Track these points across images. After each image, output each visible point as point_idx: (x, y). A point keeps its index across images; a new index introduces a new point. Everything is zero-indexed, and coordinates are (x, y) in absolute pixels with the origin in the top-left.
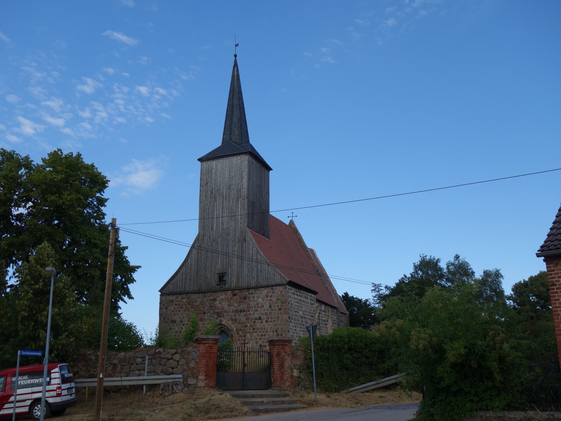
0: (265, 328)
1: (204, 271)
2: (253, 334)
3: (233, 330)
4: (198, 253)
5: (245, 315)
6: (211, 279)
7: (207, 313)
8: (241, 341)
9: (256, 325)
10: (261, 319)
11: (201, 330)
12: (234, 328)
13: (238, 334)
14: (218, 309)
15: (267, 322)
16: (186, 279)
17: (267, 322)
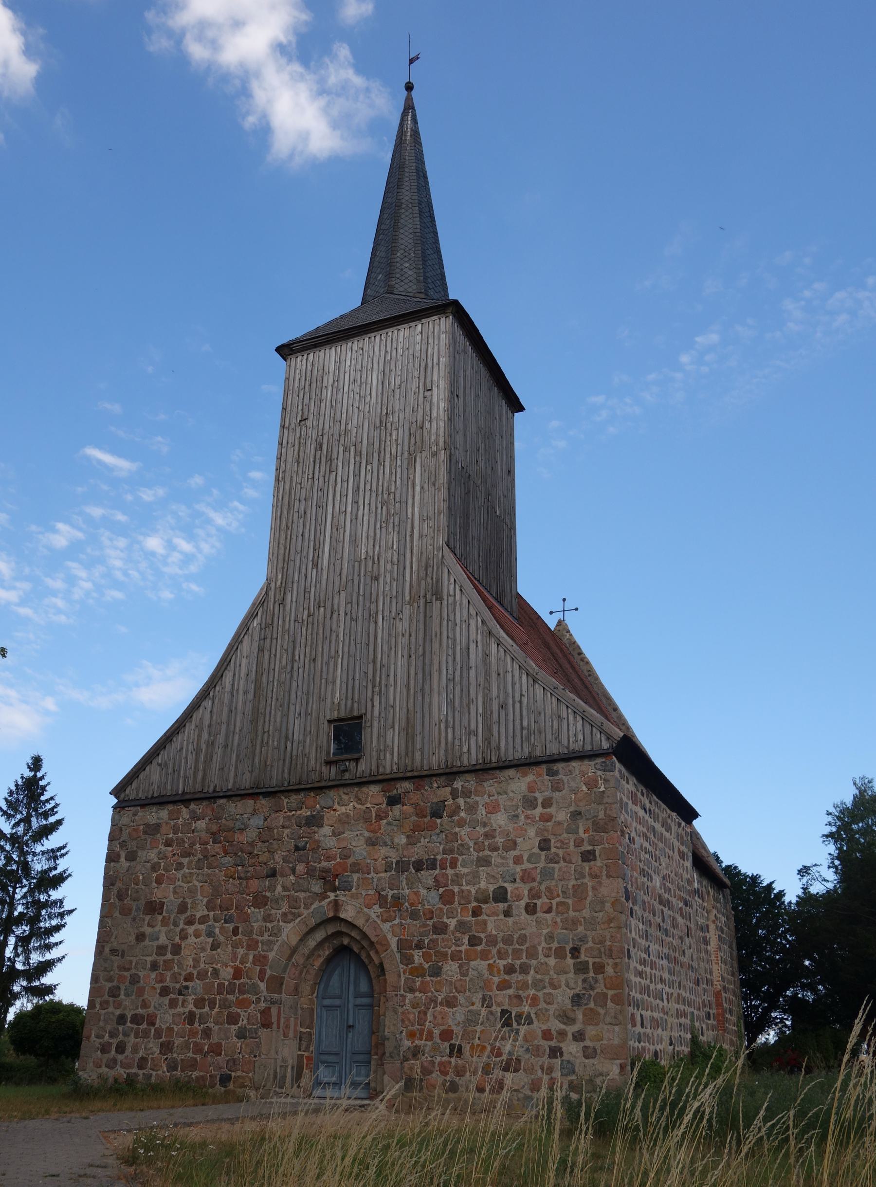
0: (523, 939)
1: (279, 714)
2: (472, 963)
3: (386, 945)
4: (261, 650)
5: (436, 880)
6: (305, 742)
7: (282, 876)
8: (417, 994)
9: (485, 923)
10: (504, 899)
11: (257, 942)
12: (389, 936)
13: (407, 960)
14: (329, 858)
15: (531, 909)
16: (211, 744)
17: (531, 909)
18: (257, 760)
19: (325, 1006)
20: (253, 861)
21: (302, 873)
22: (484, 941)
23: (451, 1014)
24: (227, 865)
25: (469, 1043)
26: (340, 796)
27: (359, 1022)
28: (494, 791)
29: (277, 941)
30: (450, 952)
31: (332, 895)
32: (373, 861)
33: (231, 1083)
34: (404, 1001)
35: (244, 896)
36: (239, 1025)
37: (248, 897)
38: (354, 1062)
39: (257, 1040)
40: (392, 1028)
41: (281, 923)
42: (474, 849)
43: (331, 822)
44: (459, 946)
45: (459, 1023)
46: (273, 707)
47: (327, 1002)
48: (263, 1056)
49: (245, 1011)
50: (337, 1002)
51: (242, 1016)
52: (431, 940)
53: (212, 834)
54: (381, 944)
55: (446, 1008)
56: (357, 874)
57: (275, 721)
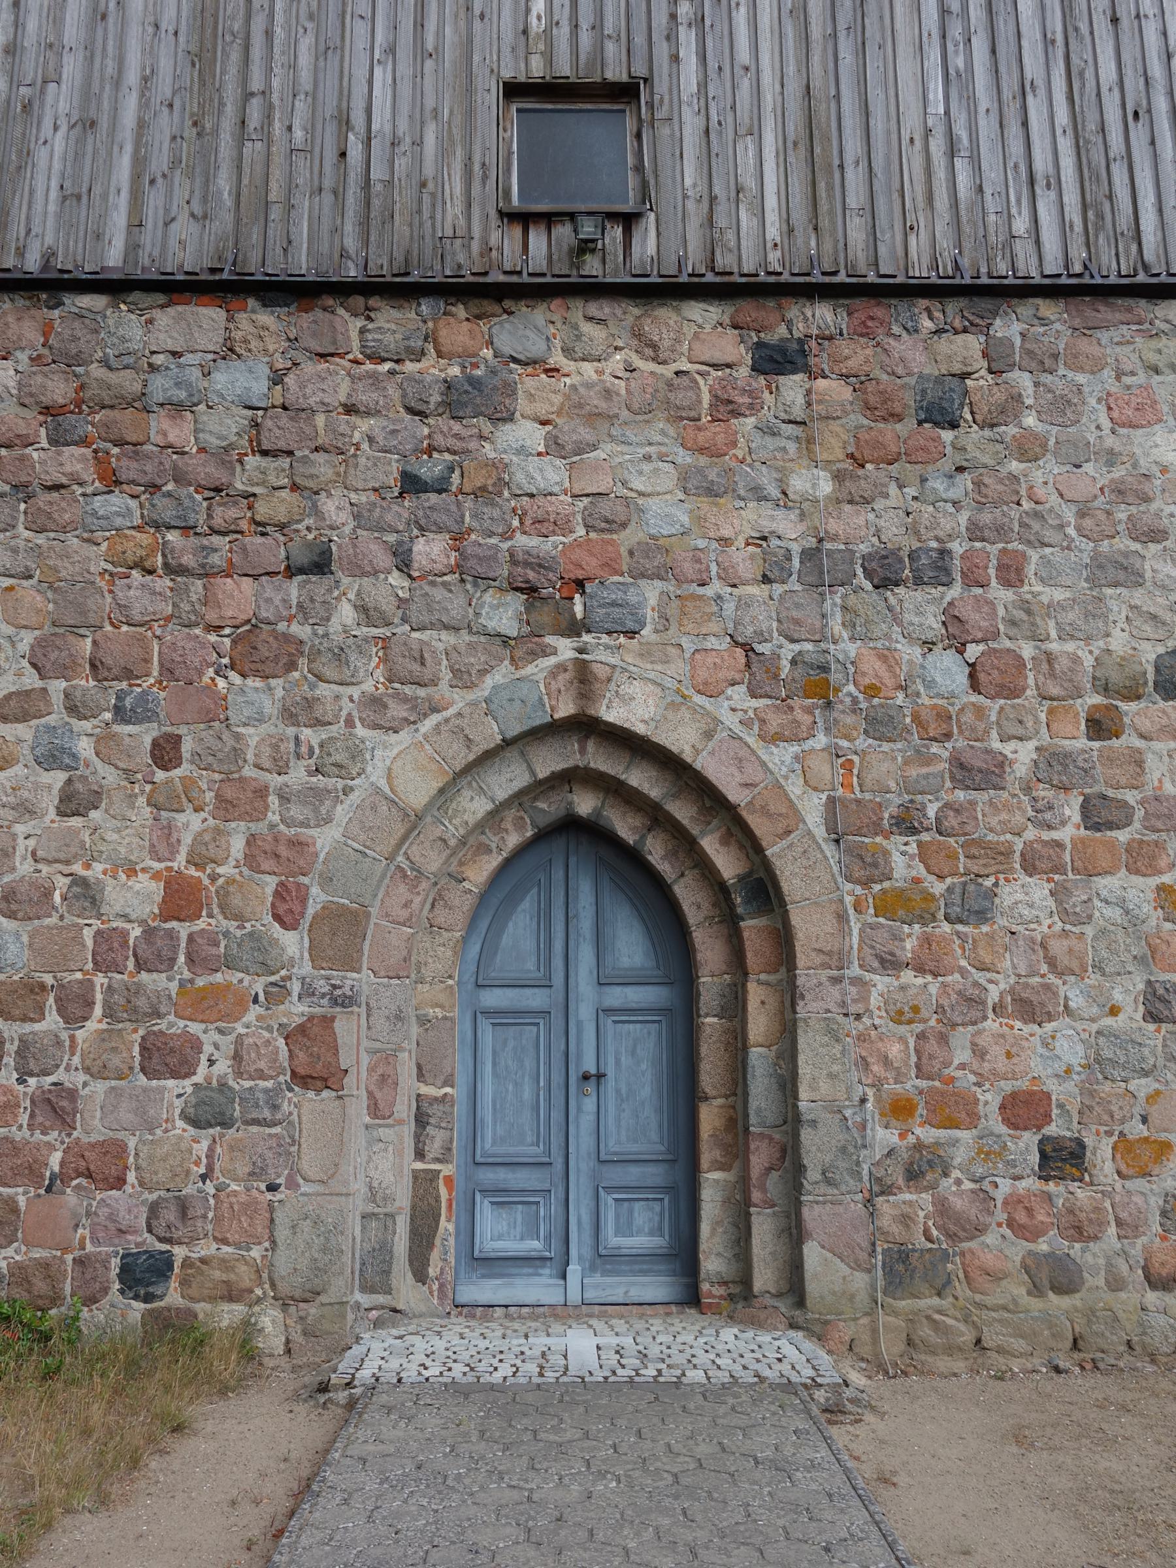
1: (306, 43)
2: (1104, 884)
5: (952, 618)
6: (419, 143)
7: (359, 570)
8: (908, 976)
9: (1137, 761)
11: (262, 792)
12: (795, 788)
14: (543, 525)
18: (224, 182)
19: (487, 1013)
20: (233, 513)
21: (439, 567)
22: (1140, 813)
23: (1036, 1040)
24: (118, 521)
25: (1109, 1134)
26: (576, 327)
27: (618, 1062)
28: (1134, 357)
29: (347, 791)
30: (1019, 847)
31: (565, 648)
32: (715, 545)
33: (174, 1284)
34: (864, 998)
35: (197, 631)
36: (198, 1078)
37: (213, 638)
38: (609, 1189)
39: (277, 1130)
40: (825, 1087)
41: (360, 731)
42: (1078, 529)
43: (542, 410)
44: (1050, 827)
45: (1068, 1071)
46: (279, 18)
47: (492, 998)
48: (305, 1188)
49: (221, 1031)
50: (535, 999)
51: (208, 1049)
52: (947, 805)
53: (47, 410)
54: (765, 811)
55: (1018, 1024)
56: (657, 583)
57: (293, 66)
